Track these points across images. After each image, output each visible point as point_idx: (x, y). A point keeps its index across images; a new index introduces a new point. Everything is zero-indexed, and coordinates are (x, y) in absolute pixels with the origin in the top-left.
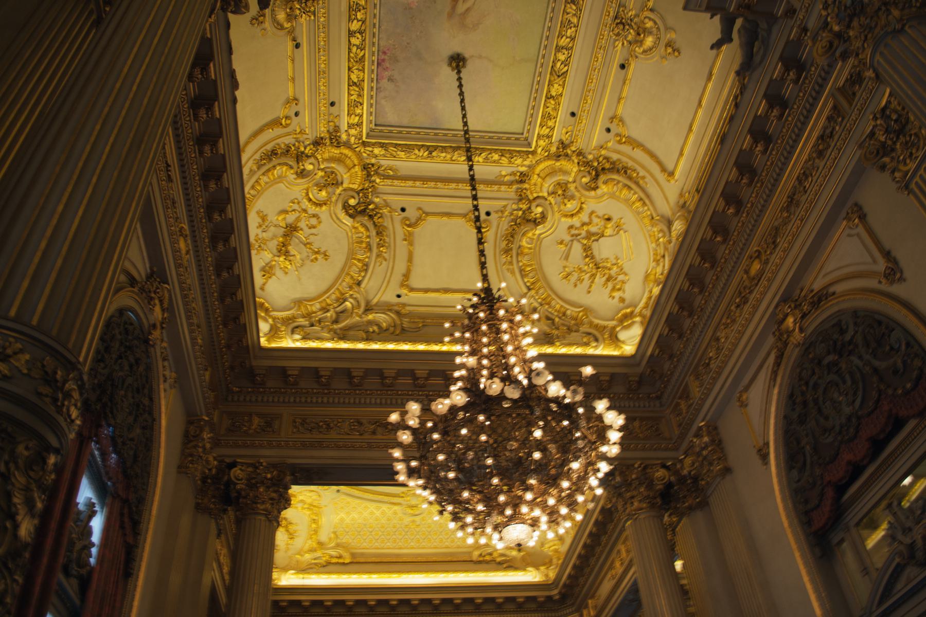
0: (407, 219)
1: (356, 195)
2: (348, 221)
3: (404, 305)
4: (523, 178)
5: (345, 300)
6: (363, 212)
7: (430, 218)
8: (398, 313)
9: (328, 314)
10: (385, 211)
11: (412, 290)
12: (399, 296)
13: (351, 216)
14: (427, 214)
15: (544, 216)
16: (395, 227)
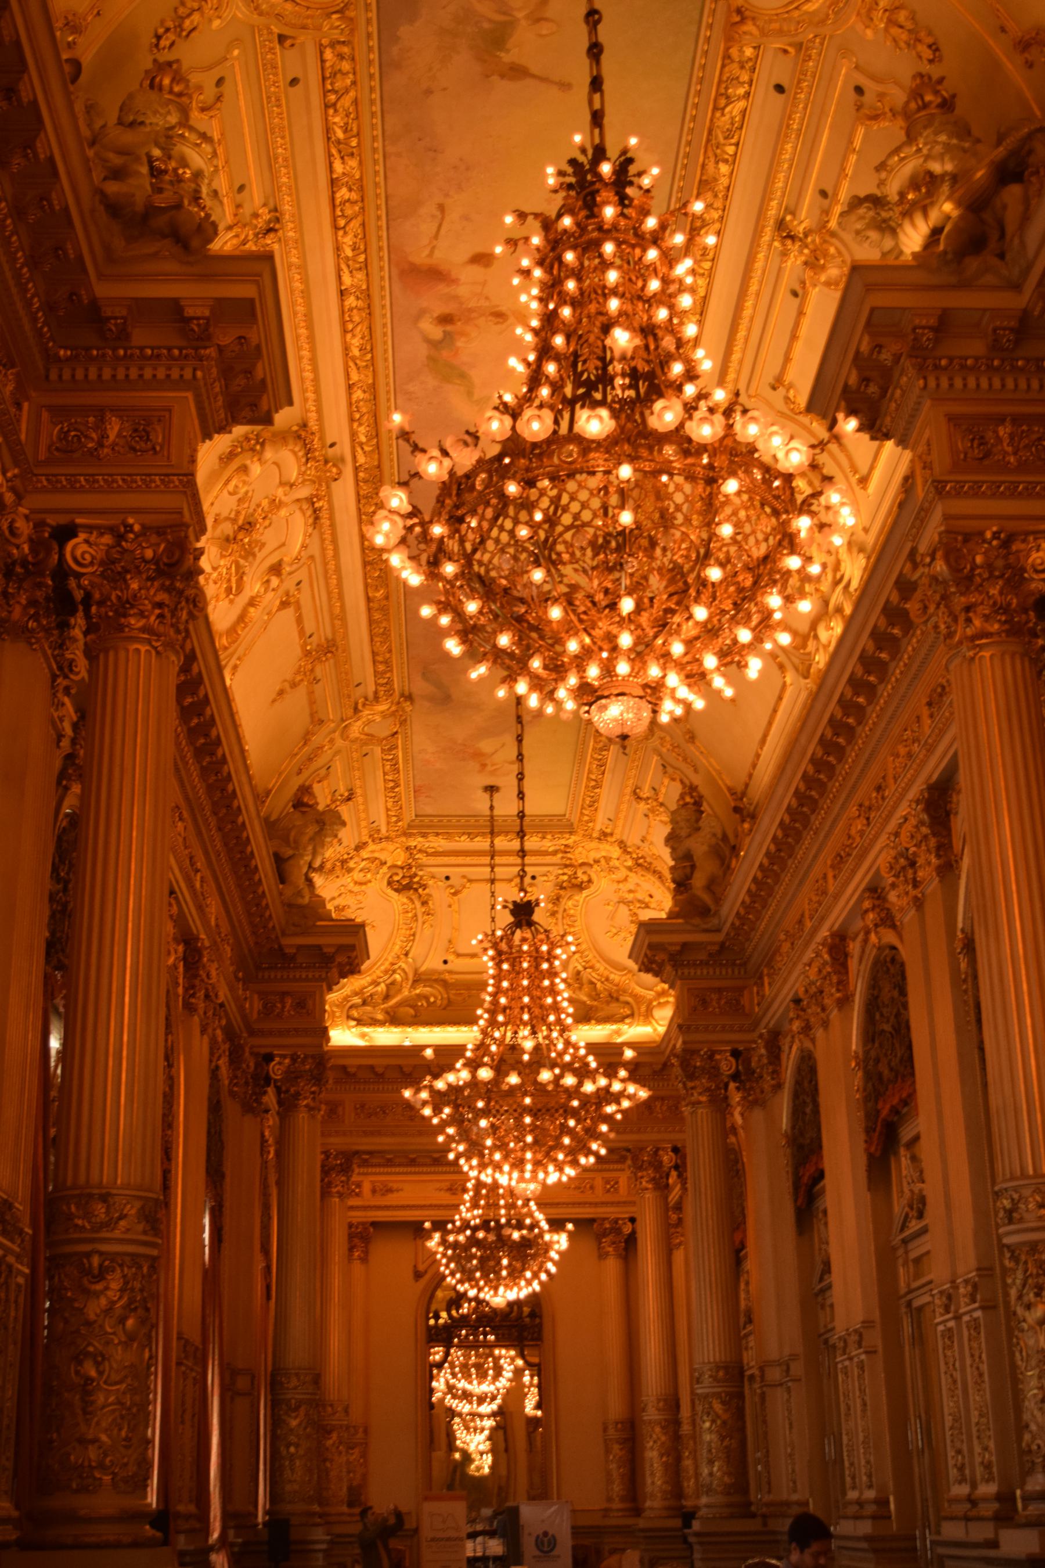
0: (452, 886)
1: (400, 872)
2: (395, 895)
3: (450, 972)
4: (566, 849)
5: (394, 972)
6: (408, 887)
7: (475, 885)
8: (445, 983)
9: (379, 989)
10: (431, 882)
11: (459, 955)
12: (445, 962)
13: (396, 890)
14: (470, 881)
15: (590, 881)
16: (438, 892)
